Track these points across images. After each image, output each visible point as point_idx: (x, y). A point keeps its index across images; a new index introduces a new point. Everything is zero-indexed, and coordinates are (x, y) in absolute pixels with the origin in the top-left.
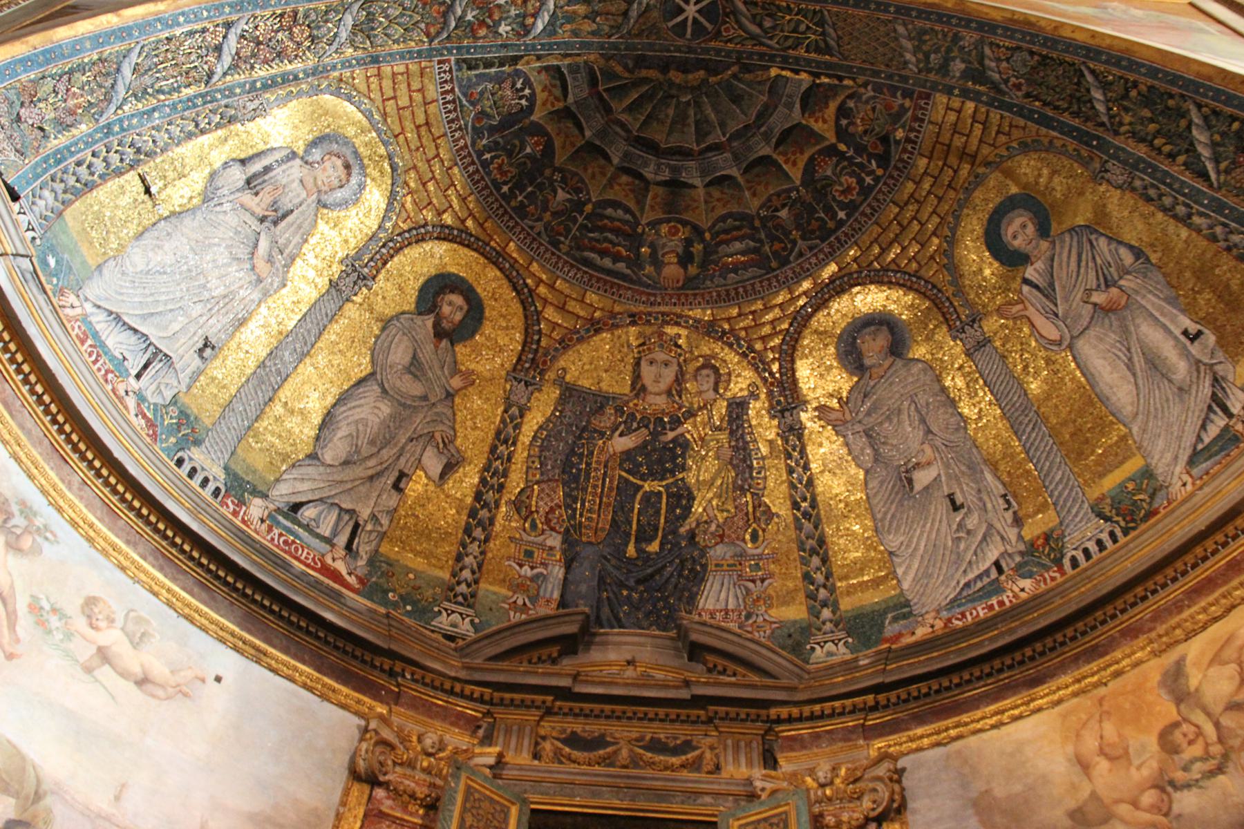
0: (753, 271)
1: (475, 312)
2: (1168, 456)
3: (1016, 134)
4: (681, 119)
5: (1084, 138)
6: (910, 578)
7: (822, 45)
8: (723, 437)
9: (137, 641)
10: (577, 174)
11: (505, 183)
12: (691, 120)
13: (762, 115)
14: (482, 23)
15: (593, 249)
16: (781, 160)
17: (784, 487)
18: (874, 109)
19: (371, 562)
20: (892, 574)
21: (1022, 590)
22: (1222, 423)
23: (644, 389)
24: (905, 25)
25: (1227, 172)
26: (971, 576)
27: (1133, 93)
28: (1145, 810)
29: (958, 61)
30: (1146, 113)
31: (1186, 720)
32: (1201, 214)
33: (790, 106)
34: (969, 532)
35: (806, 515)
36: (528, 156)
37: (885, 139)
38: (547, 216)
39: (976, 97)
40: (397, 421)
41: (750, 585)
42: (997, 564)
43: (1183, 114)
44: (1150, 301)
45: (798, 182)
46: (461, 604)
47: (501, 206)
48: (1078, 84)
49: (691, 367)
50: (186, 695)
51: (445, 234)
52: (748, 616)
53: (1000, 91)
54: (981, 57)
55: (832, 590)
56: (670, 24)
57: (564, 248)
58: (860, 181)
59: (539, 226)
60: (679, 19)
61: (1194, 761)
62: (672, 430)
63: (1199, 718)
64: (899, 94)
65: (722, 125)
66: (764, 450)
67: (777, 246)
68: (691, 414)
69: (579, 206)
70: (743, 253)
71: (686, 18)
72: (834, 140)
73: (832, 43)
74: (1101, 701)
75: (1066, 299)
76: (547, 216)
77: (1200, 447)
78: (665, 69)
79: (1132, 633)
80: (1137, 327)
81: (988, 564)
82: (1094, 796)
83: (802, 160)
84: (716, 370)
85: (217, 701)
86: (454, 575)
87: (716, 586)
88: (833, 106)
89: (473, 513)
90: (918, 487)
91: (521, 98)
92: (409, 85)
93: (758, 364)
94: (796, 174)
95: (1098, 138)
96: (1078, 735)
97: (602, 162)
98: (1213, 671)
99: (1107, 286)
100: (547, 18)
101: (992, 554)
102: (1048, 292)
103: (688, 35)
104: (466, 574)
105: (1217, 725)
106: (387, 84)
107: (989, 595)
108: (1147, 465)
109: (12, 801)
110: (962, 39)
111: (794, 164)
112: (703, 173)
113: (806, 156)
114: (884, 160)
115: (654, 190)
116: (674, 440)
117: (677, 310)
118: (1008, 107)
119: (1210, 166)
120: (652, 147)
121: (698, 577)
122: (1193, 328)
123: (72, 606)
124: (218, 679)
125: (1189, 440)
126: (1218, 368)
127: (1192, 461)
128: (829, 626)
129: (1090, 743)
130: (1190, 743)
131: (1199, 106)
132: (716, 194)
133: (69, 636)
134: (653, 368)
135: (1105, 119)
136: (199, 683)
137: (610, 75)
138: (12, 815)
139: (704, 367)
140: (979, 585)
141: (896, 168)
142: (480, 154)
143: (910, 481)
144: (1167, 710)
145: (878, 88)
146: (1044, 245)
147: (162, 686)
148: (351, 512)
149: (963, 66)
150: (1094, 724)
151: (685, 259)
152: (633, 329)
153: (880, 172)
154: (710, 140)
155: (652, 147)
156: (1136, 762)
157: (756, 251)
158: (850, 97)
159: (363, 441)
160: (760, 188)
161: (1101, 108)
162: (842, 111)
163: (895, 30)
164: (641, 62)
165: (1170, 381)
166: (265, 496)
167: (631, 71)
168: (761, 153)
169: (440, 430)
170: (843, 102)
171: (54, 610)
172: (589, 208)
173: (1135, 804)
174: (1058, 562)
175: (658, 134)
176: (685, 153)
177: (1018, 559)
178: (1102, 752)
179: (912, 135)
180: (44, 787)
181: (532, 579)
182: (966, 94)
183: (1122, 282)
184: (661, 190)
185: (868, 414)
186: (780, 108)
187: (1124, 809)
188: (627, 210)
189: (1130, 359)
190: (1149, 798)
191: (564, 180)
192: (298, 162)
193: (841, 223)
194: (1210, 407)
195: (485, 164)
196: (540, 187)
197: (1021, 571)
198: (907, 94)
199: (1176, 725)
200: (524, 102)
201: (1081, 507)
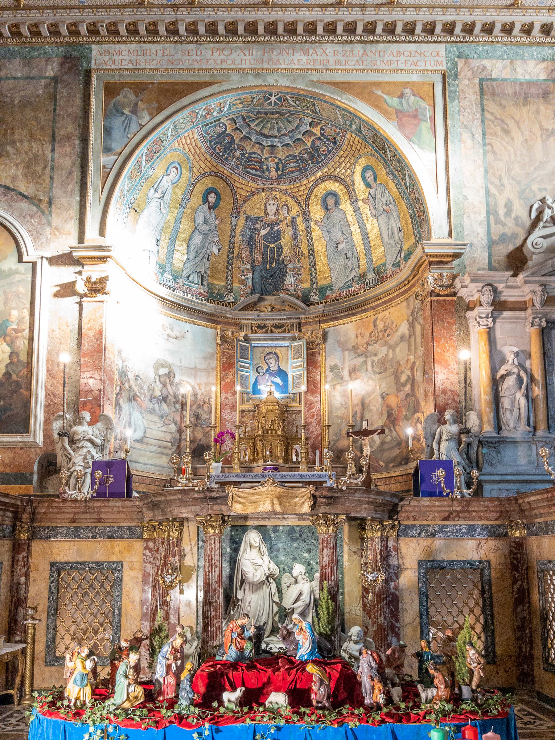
4: (272, 128)
8: (290, 228)
15: (249, 168)
16: (304, 139)
17: (306, 245)
19: (208, 286)
35: (312, 255)
36: (227, 143)
38: (234, 160)
40: (204, 240)
49: (280, 206)
54: (360, 127)
55: (316, 279)
57: (241, 168)
58: (328, 149)
59: (232, 163)
66: (301, 233)
67: (304, 165)
68: (281, 221)
69: (243, 155)
70: (294, 167)
76: (234, 160)
78: (266, 114)
83: (311, 140)
85: (189, 336)
89: (228, 263)
93: (298, 203)
94: (309, 144)
101: (352, 275)
107: (350, 287)
112: (281, 143)
114: (335, 143)
115: (266, 148)
117: (276, 186)
129: (359, 332)
132: (285, 148)
137: (249, 117)
139: (284, 205)
142: (212, 147)
144: (372, 329)
148: (200, 272)
151: (277, 170)
152: (263, 194)
154: (283, 132)
157: (298, 166)
159: (198, 249)
160: (298, 147)
169: (216, 239)
172: (247, 155)
175: (266, 131)
176: (276, 137)
184: (268, 148)
188: (258, 154)
191: (238, 147)
193: (322, 160)
196: (231, 151)
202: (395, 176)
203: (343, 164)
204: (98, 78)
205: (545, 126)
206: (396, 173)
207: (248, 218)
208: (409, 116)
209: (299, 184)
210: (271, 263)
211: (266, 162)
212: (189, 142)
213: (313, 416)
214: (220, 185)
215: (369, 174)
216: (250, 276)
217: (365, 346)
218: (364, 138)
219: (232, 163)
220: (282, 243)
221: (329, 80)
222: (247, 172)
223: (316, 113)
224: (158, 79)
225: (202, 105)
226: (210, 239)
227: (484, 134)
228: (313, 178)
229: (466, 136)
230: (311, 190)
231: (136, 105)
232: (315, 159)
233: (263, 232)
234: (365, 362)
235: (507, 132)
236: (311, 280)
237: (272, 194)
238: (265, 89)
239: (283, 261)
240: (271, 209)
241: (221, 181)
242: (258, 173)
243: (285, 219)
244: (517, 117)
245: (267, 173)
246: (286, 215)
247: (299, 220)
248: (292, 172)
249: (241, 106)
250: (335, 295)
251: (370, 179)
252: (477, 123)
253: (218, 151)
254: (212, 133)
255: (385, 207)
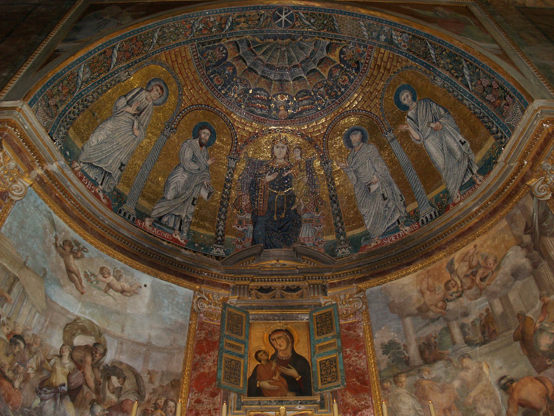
2: (454, 186)
3: (404, 63)
5: (428, 67)
6: (369, 224)
7: (333, 29)
9: (118, 278)
10: (245, 79)
11: (220, 85)
12: (286, 57)
14: (206, 29)
16: (320, 70)
18: (353, 51)
19: (188, 234)
20: (363, 225)
21: (406, 230)
22: (470, 176)
23: (275, 157)
24: (363, 22)
25: (475, 86)
26: (390, 225)
27: (444, 53)
28: (439, 308)
29: (383, 35)
30: (448, 60)
31: (453, 279)
32: (467, 100)
33: (322, 51)
34: (389, 208)
36: (228, 74)
37: (357, 62)
39: (391, 49)
41: (316, 228)
42: (398, 220)
43: (461, 63)
44: (449, 128)
45: (326, 78)
46: (220, 244)
47: (219, 94)
48: (426, 47)
50: (136, 293)
52: (316, 240)
53: (398, 47)
56: (276, 22)
58: (349, 77)
60: (280, 20)
61: (454, 293)
62: (286, 172)
63: (456, 279)
64: (362, 46)
65: (298, 58)
70: (309, 104)
71: (282, 20)
72: (339, 63)
73: (337, 28)
74: (428, 271)
75: (422, 124)
77: (463, 184)
79: (439, 249)
80: (445, 137)
81: (395, 220)
82: (425, 303)
83: (328, 70)
86: (216, 234)
87: (305, 228)
88: (338, 50)
90: (372, 191)
91: (222, 54)
92: (181, 55)
94: (326, 75)
95: (433, 68)
96: (421, 283)
97: (254, 74)
98: (461, 264)
99: (436, 121)
100: (229, 24)
101: (397, 217)
102: (415, 121)
103: (283, 26)
104: (220, 233)
105: (461, 281)
106: (173, 56)
107: (395, 232)
108: (447, 188)
109: (93, 338)
110: (384, 27)
111: (325, 71)
113: (329, 68)
114: (357, 69)
116: (287, 176)
118: (402, 53)
119: (469, 83)
120: (271, 67)
122: (463, 140)
123: (97, 272)
124: (145, 286)
125: (460, 181)
126: (470, 156)
127: (460, 189)
128: (342, 243)
130: (453, 287)
131: (466, 61)
132: (297, 83)
133: (98, 282)
134: (278, 149)
135: (435, 61)
136: (139, 289)
137: (254, 42)
138: (94, 342)
140: (392, 228)
141: (362, 72)
143: (370, 189)
145: (354, 44)
146: (415, 104)
147: (129, 292)
149: (385, 37)
150: (426, 279)
153: (356, 74)
154: (293, 64)
155: (271, 67)
156: (438, 293)
158: (344, 47)
161: (433, 57)
162: (341, 52)
163: (360, 24)
164: (267, 37)
165: (455, 158)
166: (150, 217)
167: (263, 40)
168: (312, 68)
170: (342, 50)
171: (92, 275)
172: (251, 91)
173: (436, 306)
174: (417, 221)
177: (405, 219)
178: (428, 289)
179: (367, 61)
180: (101, 332)
181: (243, 232)
182: (386, 47)
183: (441, 120)
185: (355, 164)
186: (319, 51)
189: (443, 148)
190: (440, 304)
192: (144, 91)
193: (342, 93)
194: (467, 170)
197: (406, 224)
198: (365, 47)
199: (450, 281)
200: (224, 55)
201: (425, 202)
210: (279, 213)
216: (251, 227)
217: (440, 304)
232: (333, 94)
233: (269, 178)
234: (448, 330)
243: (299, 163)
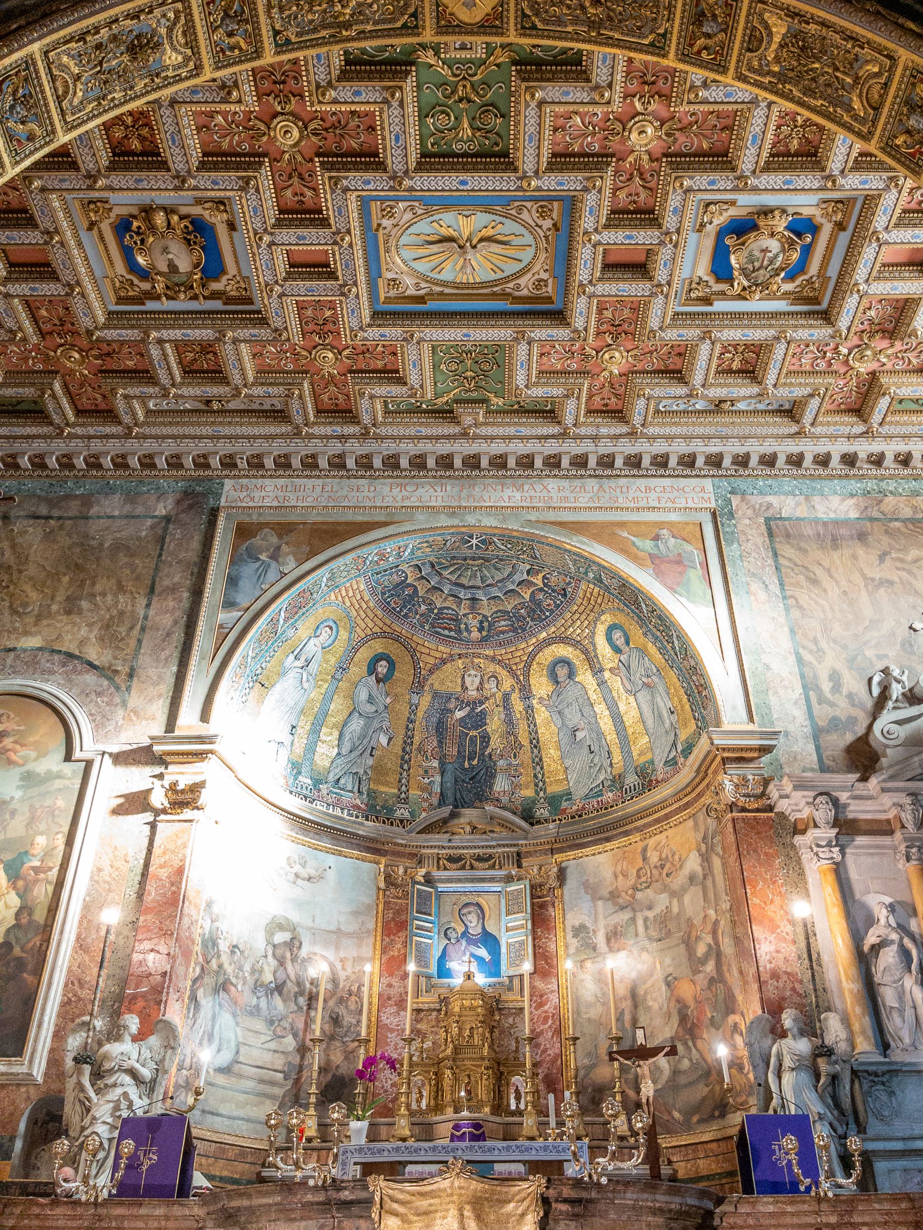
0: (511, 634)
1: (392, 665)
8: (501, 709)
13: (510, 575)
49: (486, 677)
51: (375, 636)
66: (518, 716)
68: (487, 699)
84: (496, 678)
121: (493, 776)
155: (462, 586)
164: (453, 558)
174: (622, 788)
187: (623, 894)
190: (630, 892)
195: (388, 603)
202: (657, 638)
203: (579, 622)
204: (228, 517)
205: (869, 575)
206: (658, 634)
207: (436, 695)
208: (670, 562)
209: (514, 649)
211: (465, 620)
212: (351, 594)
213: (546, 1019)
214: (394, 650)
215: (617, 635)
218: (607, 589)
219: (415, 621)
220: (489, 730)
221: (553, 519)
222: (437, 633)
223: (536, 558)
224: (313, 517)
225: (374, 549)
226: (376, 724)
227: (782, 585)
228: (534, 640)
229: (756, 586)
230: (532, 656)
231: (278, 548)
235: (815, 581)
236: (536, 785)
237: (473, 662)
238: (464, 530)
239: (490, 755)
240: (472, 682)
241: (396, 645)
242: (452, 634)
243: (494, 695)
244: (826, 563)
245: (465, 634)
246: (495, 690)
247: (515, 698)
248: (503, 632)
249: (428, 550)
250: (575, 808)
251: (620, 642)
252: (770, 570)
253: (393, 605)
254: (386, 583)
255: (644, 679)
